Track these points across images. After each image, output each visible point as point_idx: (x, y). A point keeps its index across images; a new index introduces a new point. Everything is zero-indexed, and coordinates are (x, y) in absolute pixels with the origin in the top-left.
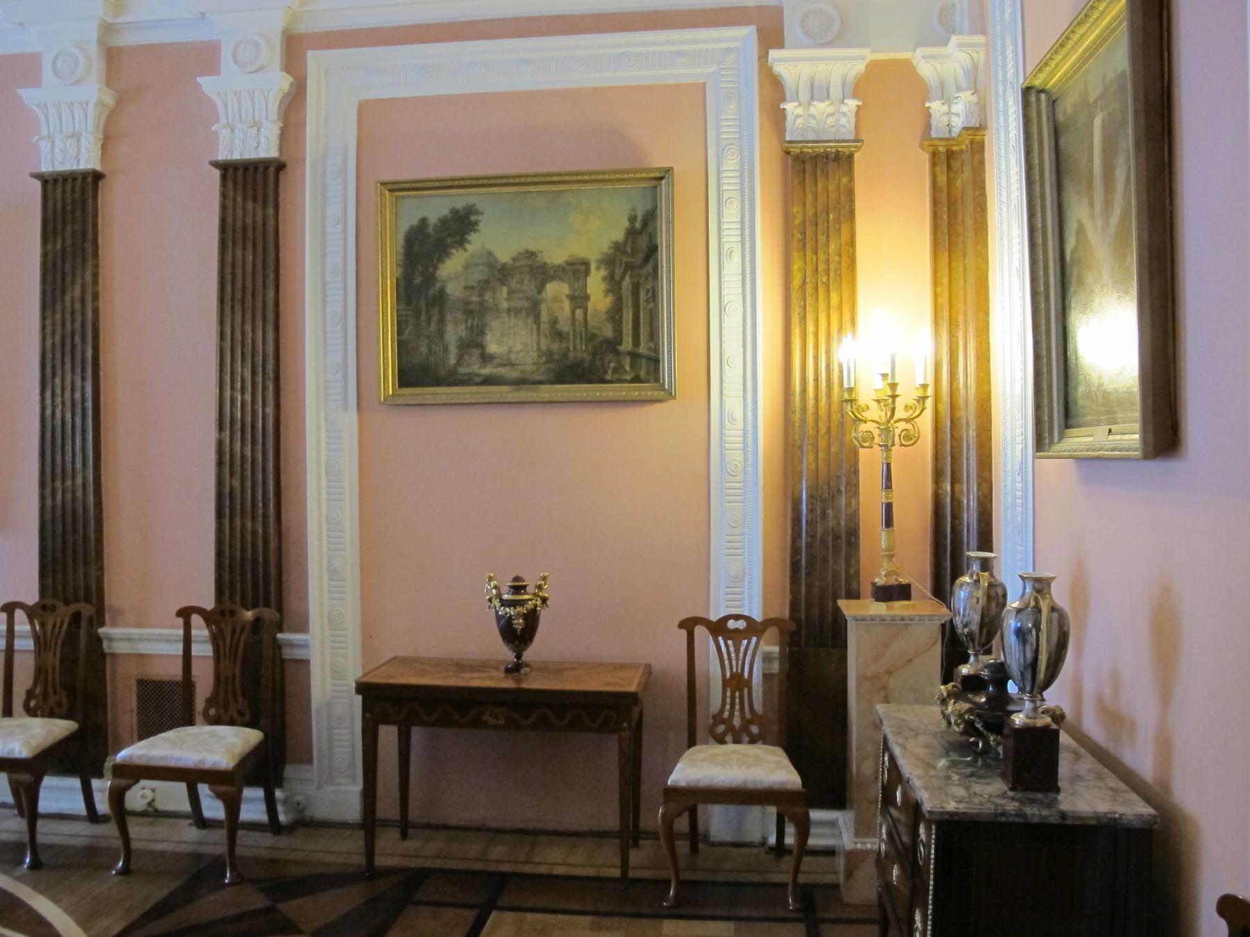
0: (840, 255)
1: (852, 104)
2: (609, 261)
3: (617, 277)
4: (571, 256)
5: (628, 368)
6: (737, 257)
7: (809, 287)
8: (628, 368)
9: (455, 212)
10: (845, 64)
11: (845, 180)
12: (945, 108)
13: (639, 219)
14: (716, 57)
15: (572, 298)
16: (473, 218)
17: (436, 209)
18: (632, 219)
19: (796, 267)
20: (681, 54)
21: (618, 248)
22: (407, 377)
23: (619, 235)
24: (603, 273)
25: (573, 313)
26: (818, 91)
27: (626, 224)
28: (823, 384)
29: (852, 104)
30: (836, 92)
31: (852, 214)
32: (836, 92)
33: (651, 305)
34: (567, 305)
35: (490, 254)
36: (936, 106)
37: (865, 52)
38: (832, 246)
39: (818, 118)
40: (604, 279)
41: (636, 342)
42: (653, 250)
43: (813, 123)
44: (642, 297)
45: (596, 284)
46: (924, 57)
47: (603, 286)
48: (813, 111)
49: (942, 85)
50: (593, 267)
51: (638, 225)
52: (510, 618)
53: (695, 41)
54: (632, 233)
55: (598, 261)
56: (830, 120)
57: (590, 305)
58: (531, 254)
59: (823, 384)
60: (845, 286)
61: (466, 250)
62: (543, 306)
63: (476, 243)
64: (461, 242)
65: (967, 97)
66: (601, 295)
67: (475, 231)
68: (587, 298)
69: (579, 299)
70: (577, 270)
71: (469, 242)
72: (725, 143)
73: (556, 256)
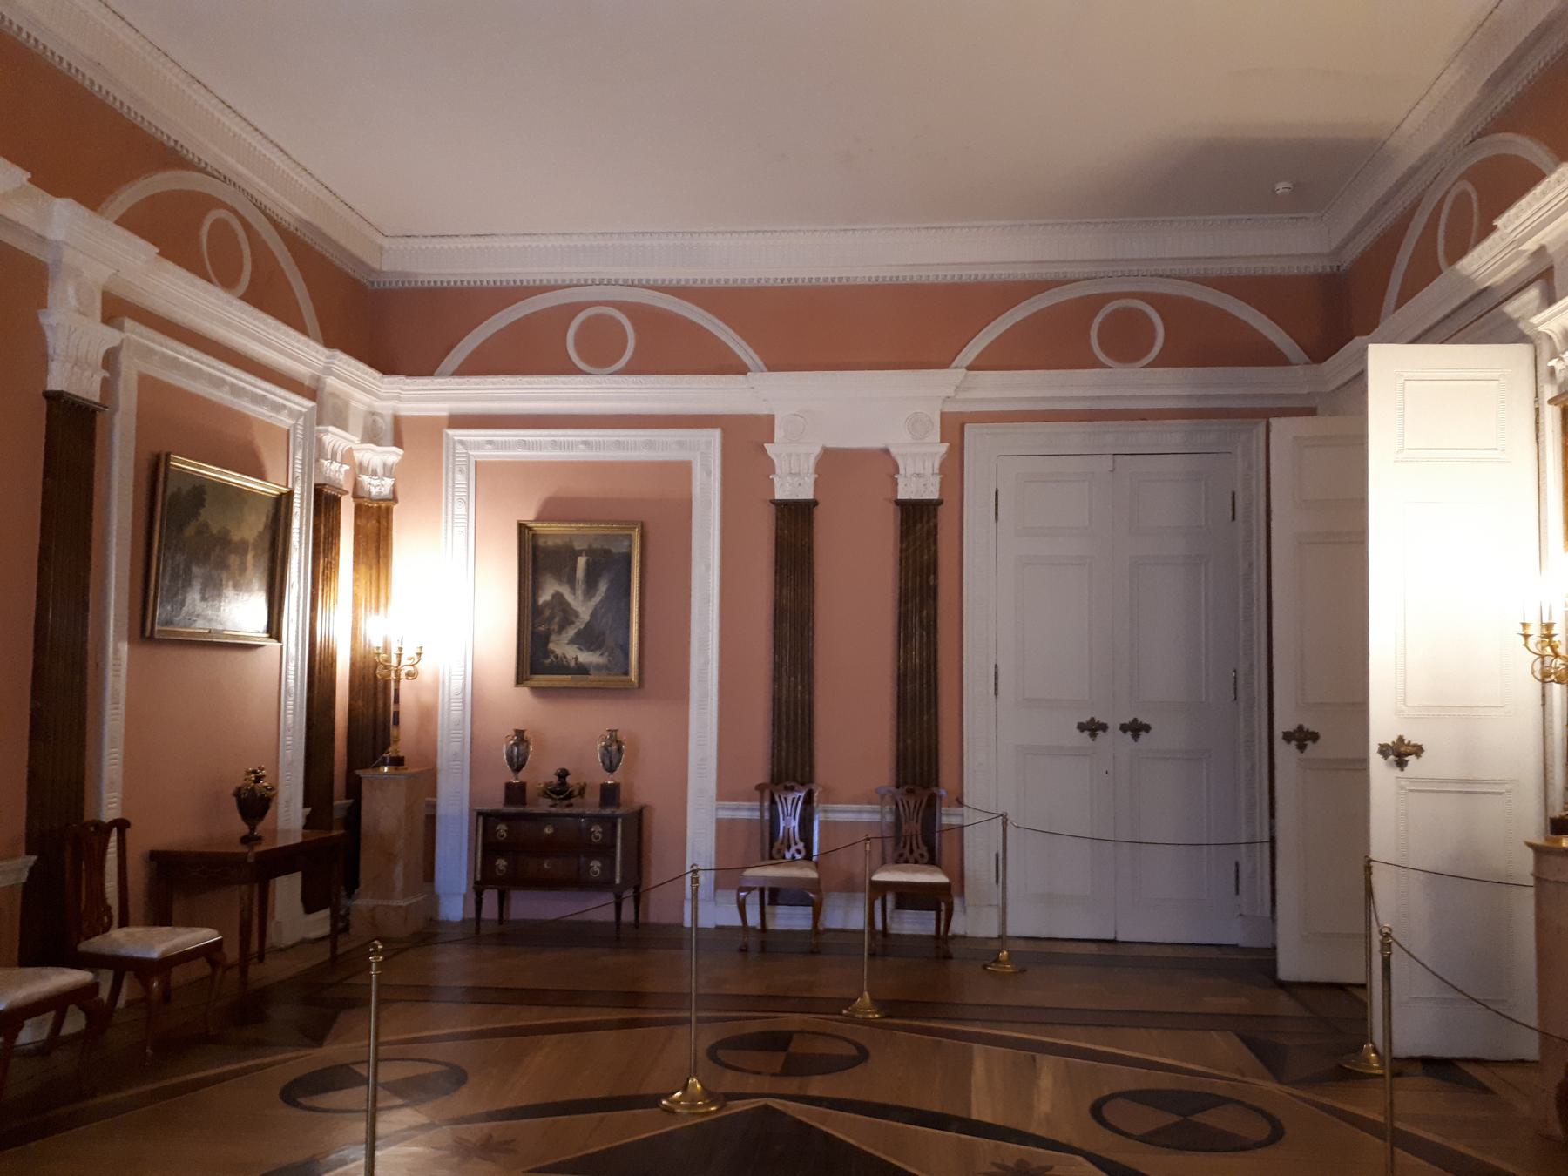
26: (334, 458)
39: (336, 472)
65: (389, 482)
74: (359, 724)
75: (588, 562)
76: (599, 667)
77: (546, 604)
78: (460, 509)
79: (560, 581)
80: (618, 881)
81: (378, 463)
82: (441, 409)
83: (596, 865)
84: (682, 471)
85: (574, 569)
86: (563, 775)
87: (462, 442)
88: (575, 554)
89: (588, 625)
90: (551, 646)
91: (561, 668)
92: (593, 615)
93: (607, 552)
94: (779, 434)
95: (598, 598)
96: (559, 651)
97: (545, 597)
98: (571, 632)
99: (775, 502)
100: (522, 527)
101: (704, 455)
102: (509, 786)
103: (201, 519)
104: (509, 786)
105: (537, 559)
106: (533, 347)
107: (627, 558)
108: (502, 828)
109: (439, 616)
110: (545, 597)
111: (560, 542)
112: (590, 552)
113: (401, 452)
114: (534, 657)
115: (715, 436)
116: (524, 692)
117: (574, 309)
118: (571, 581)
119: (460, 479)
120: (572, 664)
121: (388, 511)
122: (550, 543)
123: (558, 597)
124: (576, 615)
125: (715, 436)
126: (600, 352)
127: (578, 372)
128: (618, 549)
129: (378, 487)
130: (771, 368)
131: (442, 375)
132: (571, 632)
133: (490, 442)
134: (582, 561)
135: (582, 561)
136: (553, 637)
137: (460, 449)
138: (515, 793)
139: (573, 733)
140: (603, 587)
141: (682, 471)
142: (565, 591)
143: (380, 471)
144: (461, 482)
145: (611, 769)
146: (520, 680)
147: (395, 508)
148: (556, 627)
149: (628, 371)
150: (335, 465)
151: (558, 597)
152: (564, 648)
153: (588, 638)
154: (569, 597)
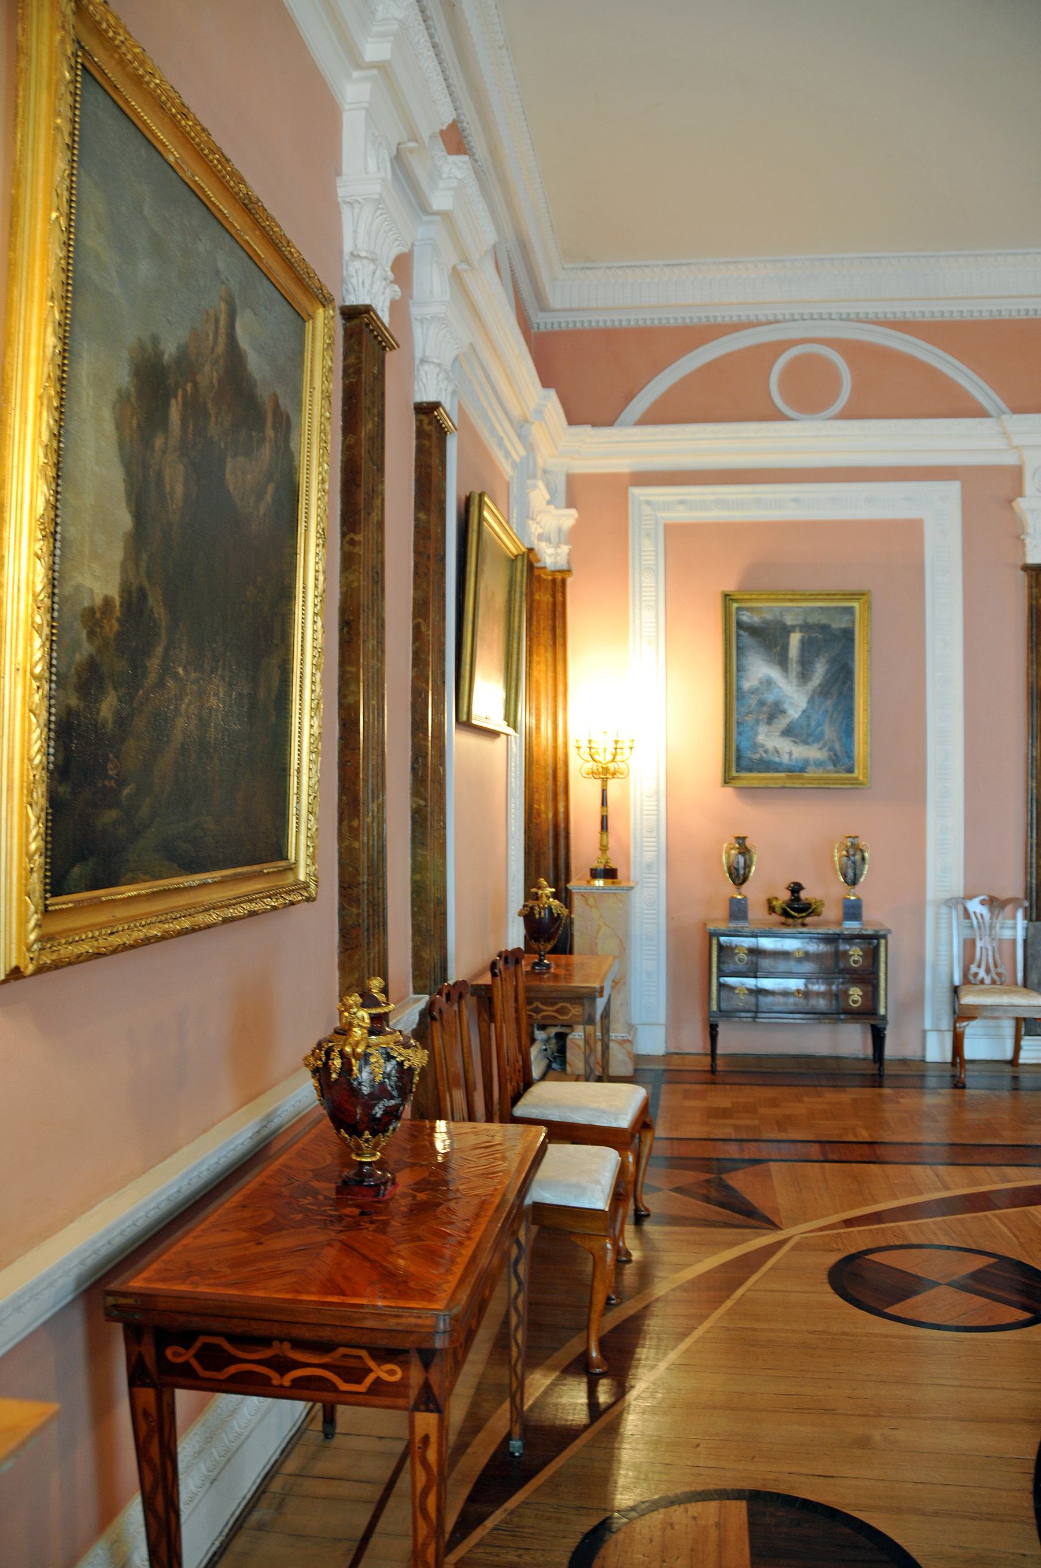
65: (565, 549)
75: (802, 641)
76: (819, 764)
78: (648, 581)
79: (770, 661)
82: (623, 465)
84: (911, 531)
85: (785, 648)
86: (796, 889)
87: (648, 503)
93: (824, 628)
94: (1029, 486)
99: (1027, 568)
100: (727, 597)
101: (940, 518)
106: (731, 392)
112: (805, 627)
115: (953, 489)
116: (729, 791)
117: (780, 347)
118: (783, 662)
119: (647, 545)
121: (564, 582)
125: (953, 489)
126: (811, 393)
127: (782, 417)
130: (1017, 410)
131: (624, 424)
133: (682, 502)
134: (795, 638)
135: (795, 638)
137: (647, 510)
139: (793, 840)
141: (913, 529)
142: (774, 673)
143: (554, 537)
144: (647, 553)
146: (727, 780)
147: (569, 581)
149: (846, 415)
152: (770, 740)
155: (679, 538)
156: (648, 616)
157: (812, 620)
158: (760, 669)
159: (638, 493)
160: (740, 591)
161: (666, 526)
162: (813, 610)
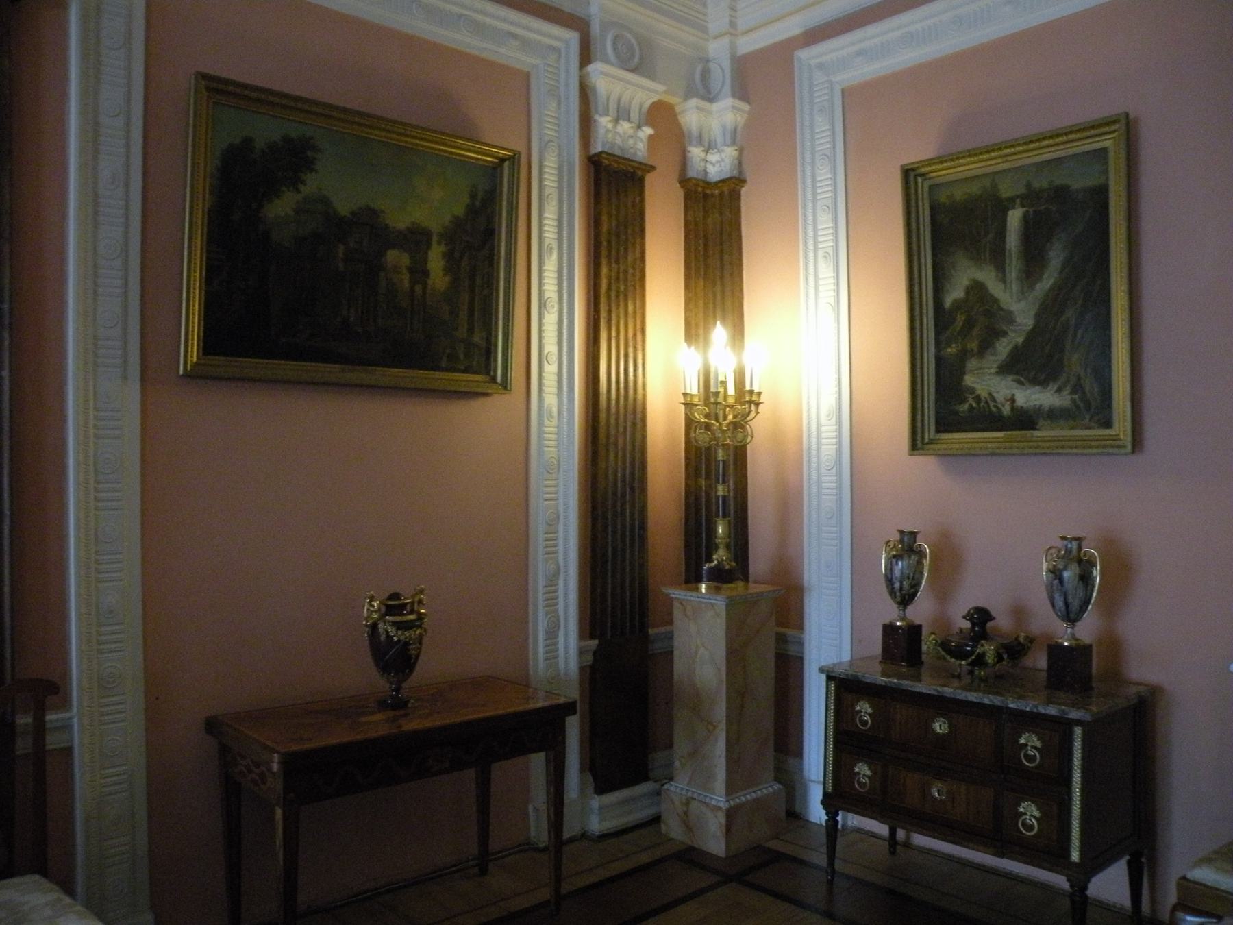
0: (634, 268)
1: (648, 131)
2: (451, 236)
3: (457, 255)
4: (413, 223)
5: (462, 357)
6: (554, 256)
7: (613, 294)
8: (462, 357)
9: (287, 140)
10: (641, 92)
11: (638, 200)
12: (703, 155)
13: (479, 198)
14: (534, 46)
15: (411, 270)
16: (309, 153)
17: (266, 131)
18: (473, 196)
19: (604, 271)
20: (515, 36)
21: (458, 223)
22: (216, 340)
23: (459, 210)
24: (443, 248)
25: (412, 290)
26: (622, 114)
27: (466, 200)
28: (622, 385)
29: (648, 131)
30: (634, 115)
31: (643, 230)
32: (634, 115)
33: (485, 292)
34: (406, 277)
35: (326, 202)
36: (695, 152)
37: (661, 88)
38: (630, 259)
39: (625, 136)
40: (444, 255)
41: (471, 330)
42: (490, 233)
43: (619, 141)
44: (478, 282)
45: (436, 260)
46: (698, 108)
47: (442, 263)
48: (620, 129)
49: (700, 136)
50: (435, 239)
51: (478, 203)
52: (407, 644)
53: (527, 28)
54: (473, 211)
55: (441, 235)
56: (631, 142)
57: (430, 282)
58: (372, 213)
59: (622, 385)
60: (638, 297)
61: (298, 191)
62: (382, 274)
63: (312, 184)
64: (295, 183)
65: (730, 153)
66: (441, 273)
67: (312, 170)
68: (426, 273)
69: (419, 272)
70: (416, 239)
71: (303, 182)
72: (547, 138)
73: (399, 221)
74: (673, 518)
75: (1025, 219)
76: (1053, 415)
77: (957, 305)
79: (977, 259)
80: (1075, 856)
81: (715, 134)
83: (1030, 811)
87: (821, 66)
88: (1001, 207)
89: (1032, 335)
90: (969, 380)
91: (988, 418)
92: (1039, 317)
93: (1060, 193)
95: (1047, 282)
96: (981, 390)
97: (955, 293)
98: (1003, 348)
100: (908, 174)
102: (889, 630)
103: (306, 190)
104: (889, 630)
105: (946, 229)
107: (1101, 194)
108: (864, 708)
109: (804, 350)
110: (955, 293)
111: (975, 189)
112: (1030, 197)
113: (746, 107)
114: (944, 405)
116: (926, 464)
118: (998, 257)
120: (1006, 410)
121: (735, 196)
122: (959, 194)
123: (977, 289)
124: (1010, 318)
128: (1079, 182)
129: (715, 164)
132: (1003, 348)
133: (859, 53)
134: (1015, 217)
135: (1015, 217)
136: (972, 364)
138: (902, 644)
140: (1056, 257)
142: (987, 276)
144: (820, 134)
145: (1071, 616)
147: (743, 191)
148: (973, 345)
150: (625, 127)
151: (977, 289)
152: (987, 382)
153: (1031, 363)
154: (995, 288)
155: (858, 101)
156: (825, 221)
157: (1041, 183)
158: (965, 275)
159: (805, 55)
160: (940, 160)
161: (843, 91)
162: (1041, 166)
